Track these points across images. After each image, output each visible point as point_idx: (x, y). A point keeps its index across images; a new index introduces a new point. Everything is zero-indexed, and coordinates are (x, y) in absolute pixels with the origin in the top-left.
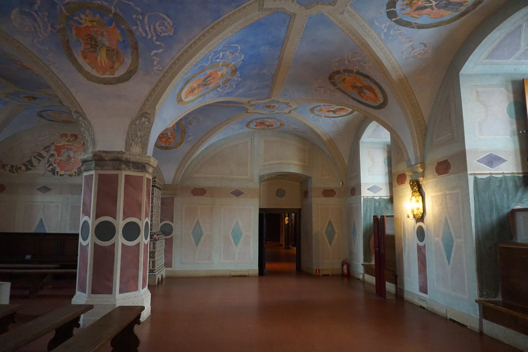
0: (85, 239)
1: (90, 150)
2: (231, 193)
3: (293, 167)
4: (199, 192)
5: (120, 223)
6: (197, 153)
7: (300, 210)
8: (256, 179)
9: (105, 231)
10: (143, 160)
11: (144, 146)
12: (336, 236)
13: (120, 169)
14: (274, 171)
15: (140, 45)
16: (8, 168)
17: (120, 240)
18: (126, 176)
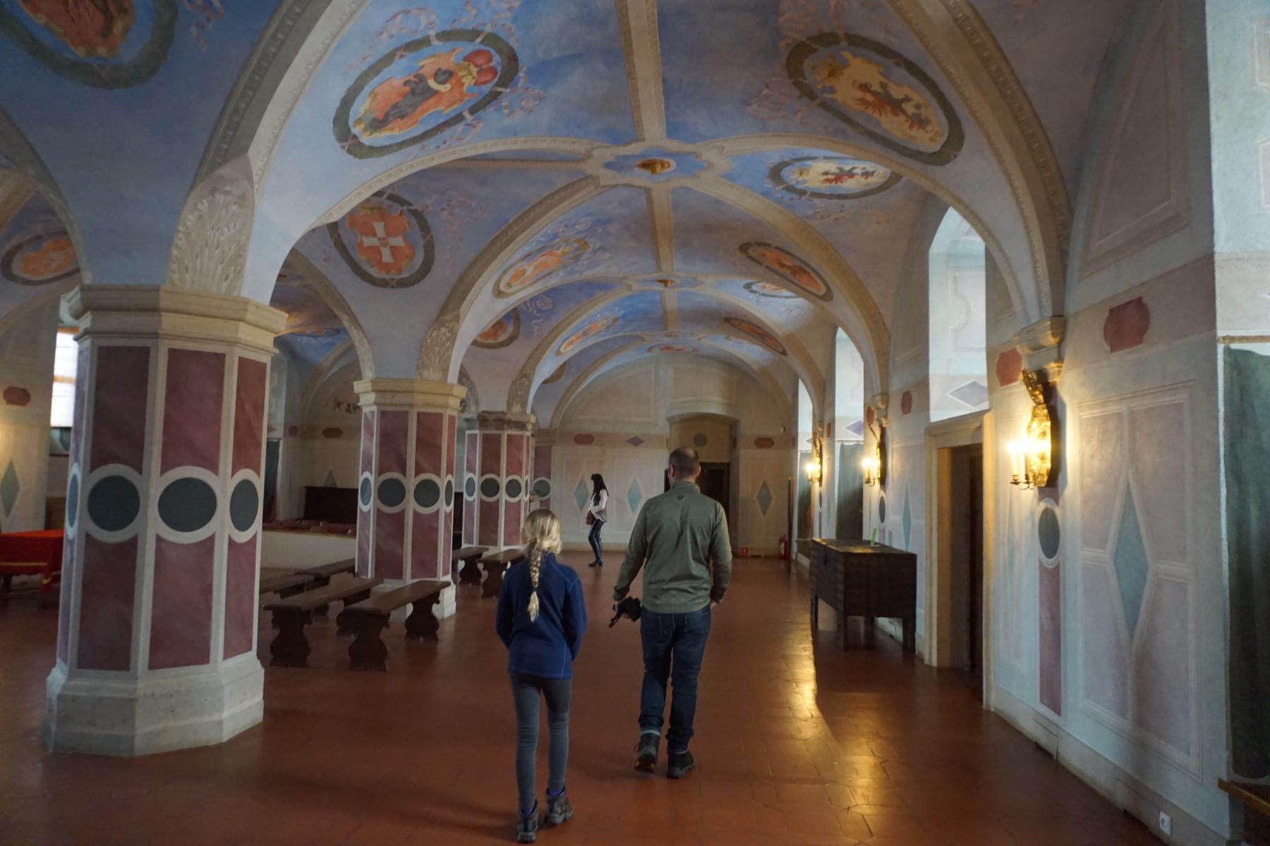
0: (471, 495)
1: (473, 409)
2: (629, 441)
3: (715, 406)
4: (585, 439)
5: (503, 481)
6: (583, 386)
7: (728, 464)
8: (662, 421)
9: (490, 488)
10: (524, 419)
11: (524, 404)
12: (773, 504)
13: (502, 429)
14: (686, 412)
15: (522, 317)
16: (344, 407)
17: (503, 496)
18: (509, 436)
